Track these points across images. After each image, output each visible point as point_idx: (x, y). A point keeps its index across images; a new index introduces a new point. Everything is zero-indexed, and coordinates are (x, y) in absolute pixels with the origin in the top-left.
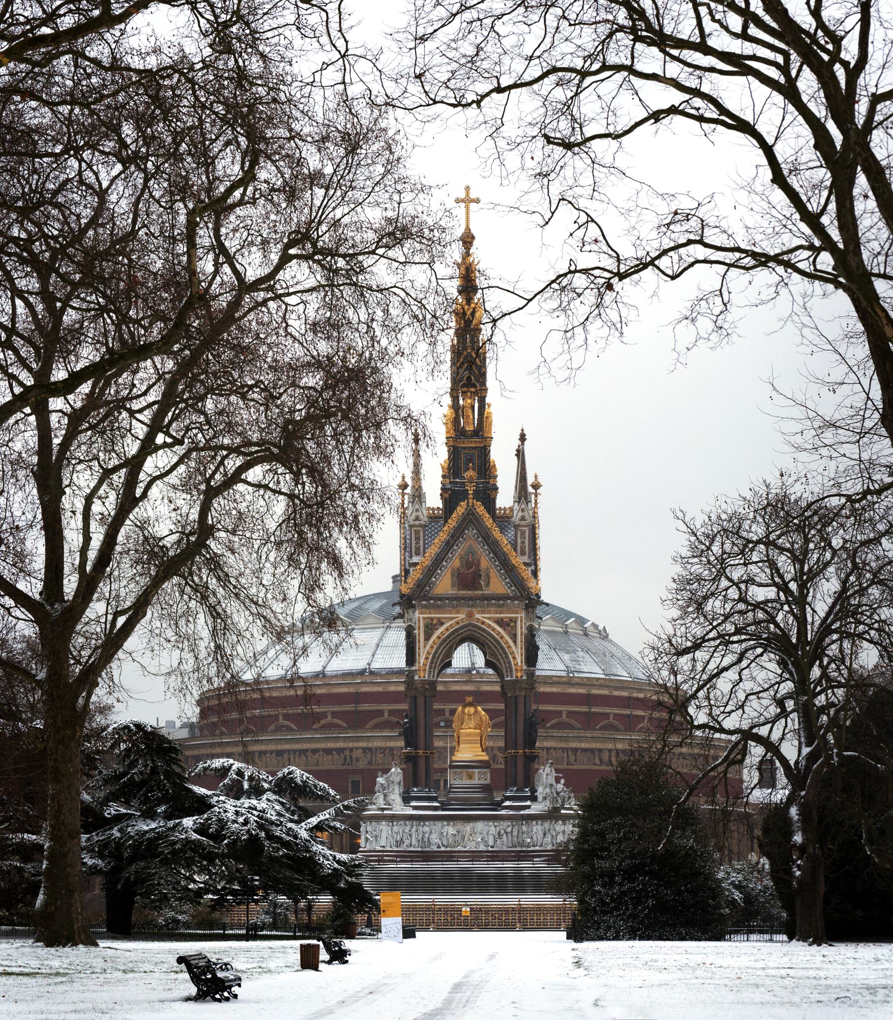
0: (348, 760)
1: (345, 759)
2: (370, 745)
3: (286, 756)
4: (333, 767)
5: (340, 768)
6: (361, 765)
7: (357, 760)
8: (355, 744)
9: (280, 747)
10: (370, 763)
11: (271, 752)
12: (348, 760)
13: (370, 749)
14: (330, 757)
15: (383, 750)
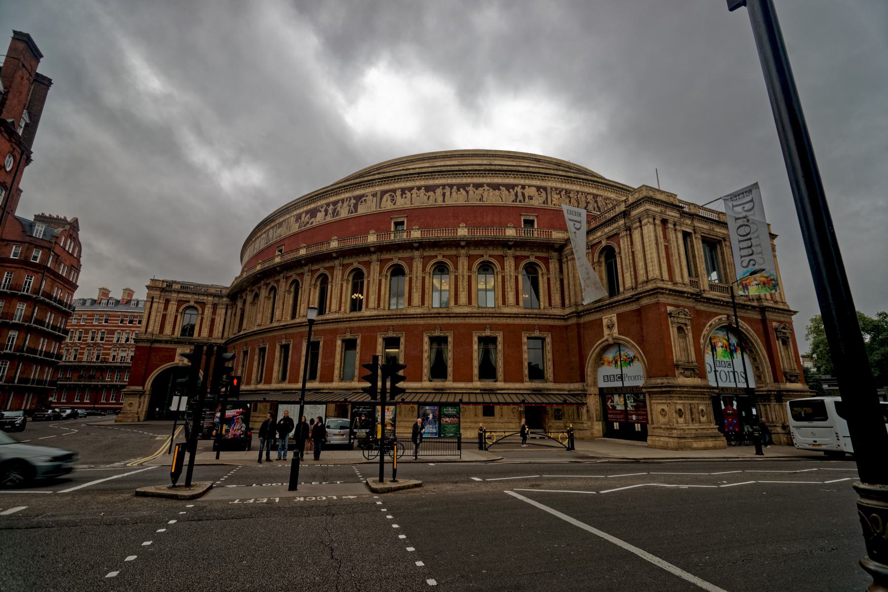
0: (520, 197)
1: (516, 195)
2: (544, 184)
3: (439, 191)
4: (499, 202)
5: (509, 203)
6: (537, 202)
7: (531, 198)
8: (527, 182)
9: (431, 182)
10: (544, 203)
11: (419, 188)
12: (520, 197)
13: (545, 189)
14: (497, 192)
15: (559, 191)
